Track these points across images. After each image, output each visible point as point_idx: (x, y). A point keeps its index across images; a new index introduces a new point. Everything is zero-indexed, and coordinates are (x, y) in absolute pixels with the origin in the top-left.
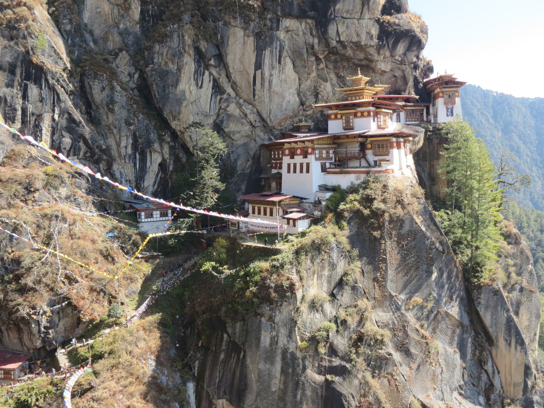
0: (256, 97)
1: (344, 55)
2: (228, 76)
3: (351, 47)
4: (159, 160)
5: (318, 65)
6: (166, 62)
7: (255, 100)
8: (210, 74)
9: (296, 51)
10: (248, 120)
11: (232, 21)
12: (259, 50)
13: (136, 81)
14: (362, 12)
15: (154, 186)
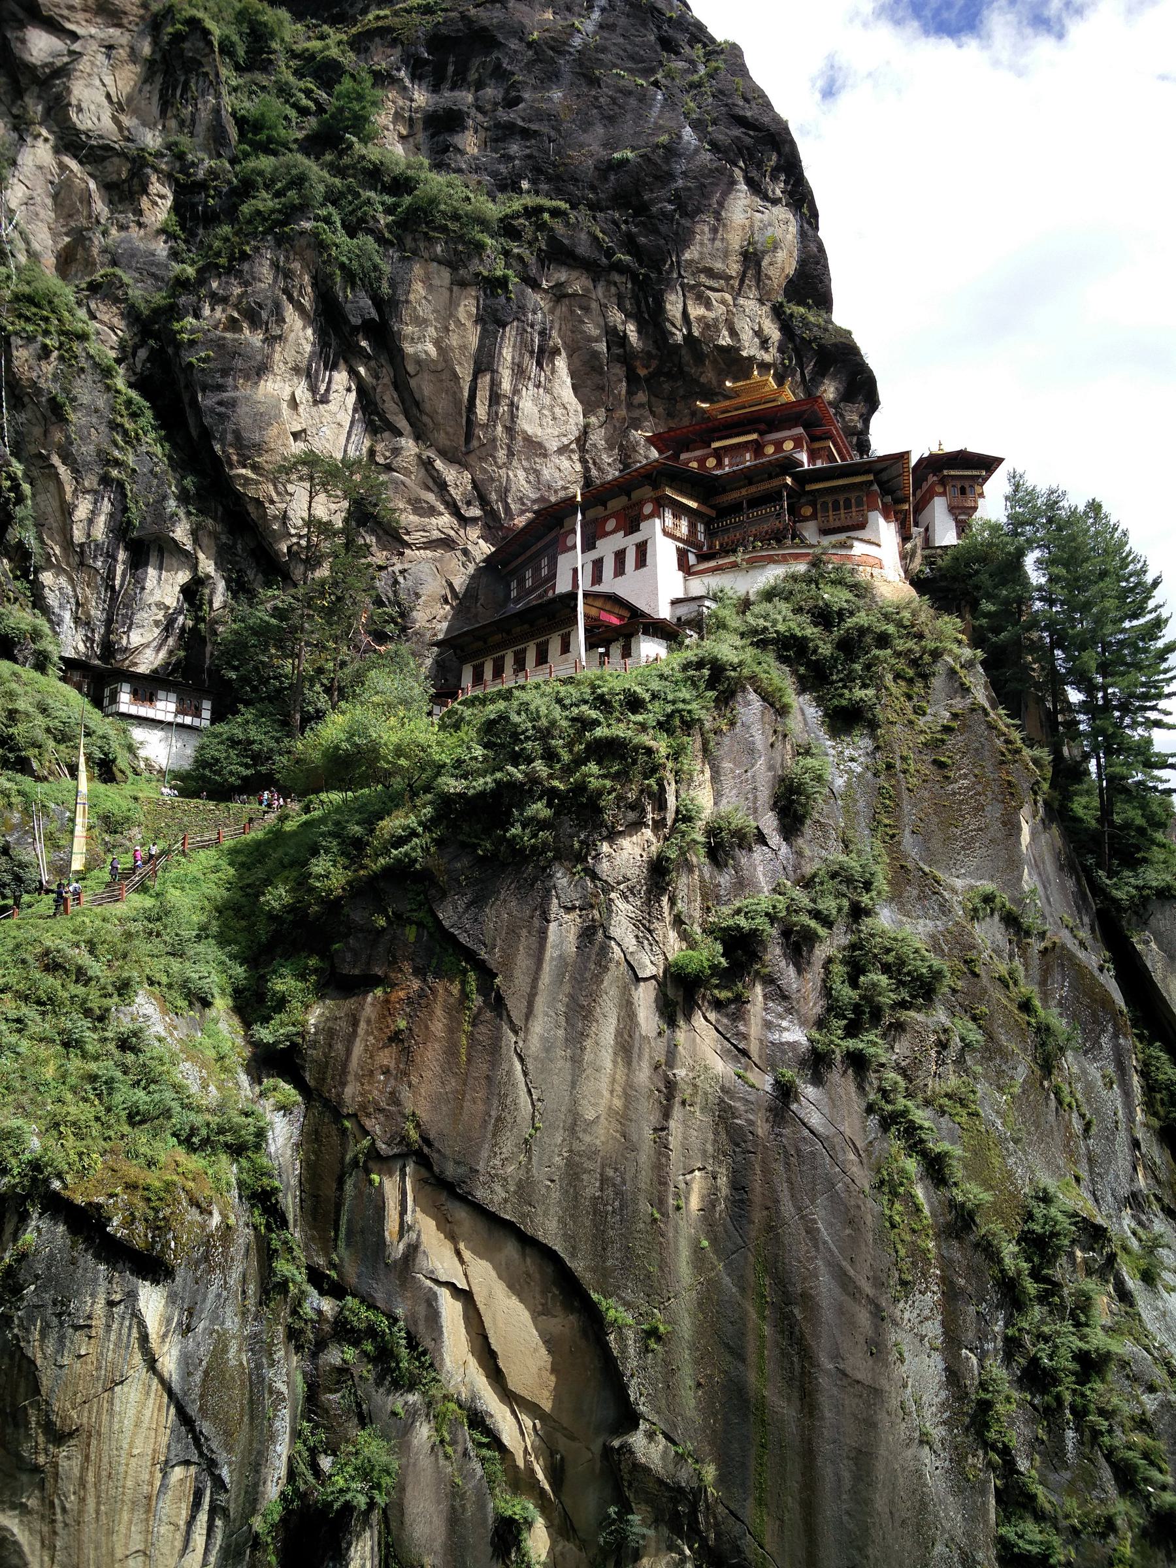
0: (475, 443)
1: (697, 382)
2: (401, 385)
3: (715, 361)
4: (183, 577)
5: (630, 393)
6: (232, 320)
7: (468, 453)
8: (353, 373)
9: (579, 348)
10: (447, 498)
11: (422, 245)
12: (492, 321)
13: (138, 370)
14: (742, 282)
15: (158, 649)
